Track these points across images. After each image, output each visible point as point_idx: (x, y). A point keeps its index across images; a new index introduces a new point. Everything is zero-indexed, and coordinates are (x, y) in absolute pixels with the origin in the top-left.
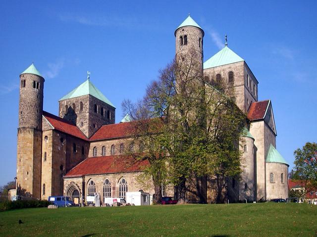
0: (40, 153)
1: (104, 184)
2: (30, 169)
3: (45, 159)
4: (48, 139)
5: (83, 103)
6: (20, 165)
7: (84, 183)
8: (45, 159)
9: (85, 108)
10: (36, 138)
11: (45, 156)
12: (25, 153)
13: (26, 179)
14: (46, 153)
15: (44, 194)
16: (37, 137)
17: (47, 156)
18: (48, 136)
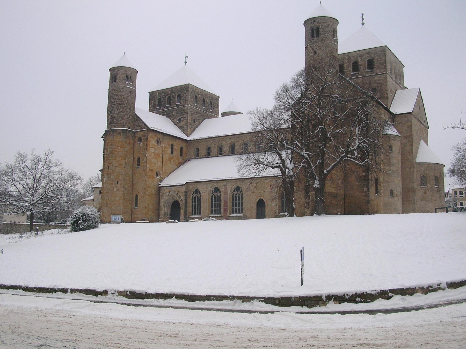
0: (132, 158)
1: (212, 193)
2: (121, 178)
3: (138, 165)
4: (142, 141)
5: (181, 94)
6: (108, 174)
7: (186, 192)
8: (138, 165)
9: (184, 101)
10: (128, 140)
11: (139, 162)
12: (115, 159)
13: (115, 190)
14: (139, 158)
15: (136, 206)
16: (129, 139)
17: (141, 161)
18: (142, 138)
